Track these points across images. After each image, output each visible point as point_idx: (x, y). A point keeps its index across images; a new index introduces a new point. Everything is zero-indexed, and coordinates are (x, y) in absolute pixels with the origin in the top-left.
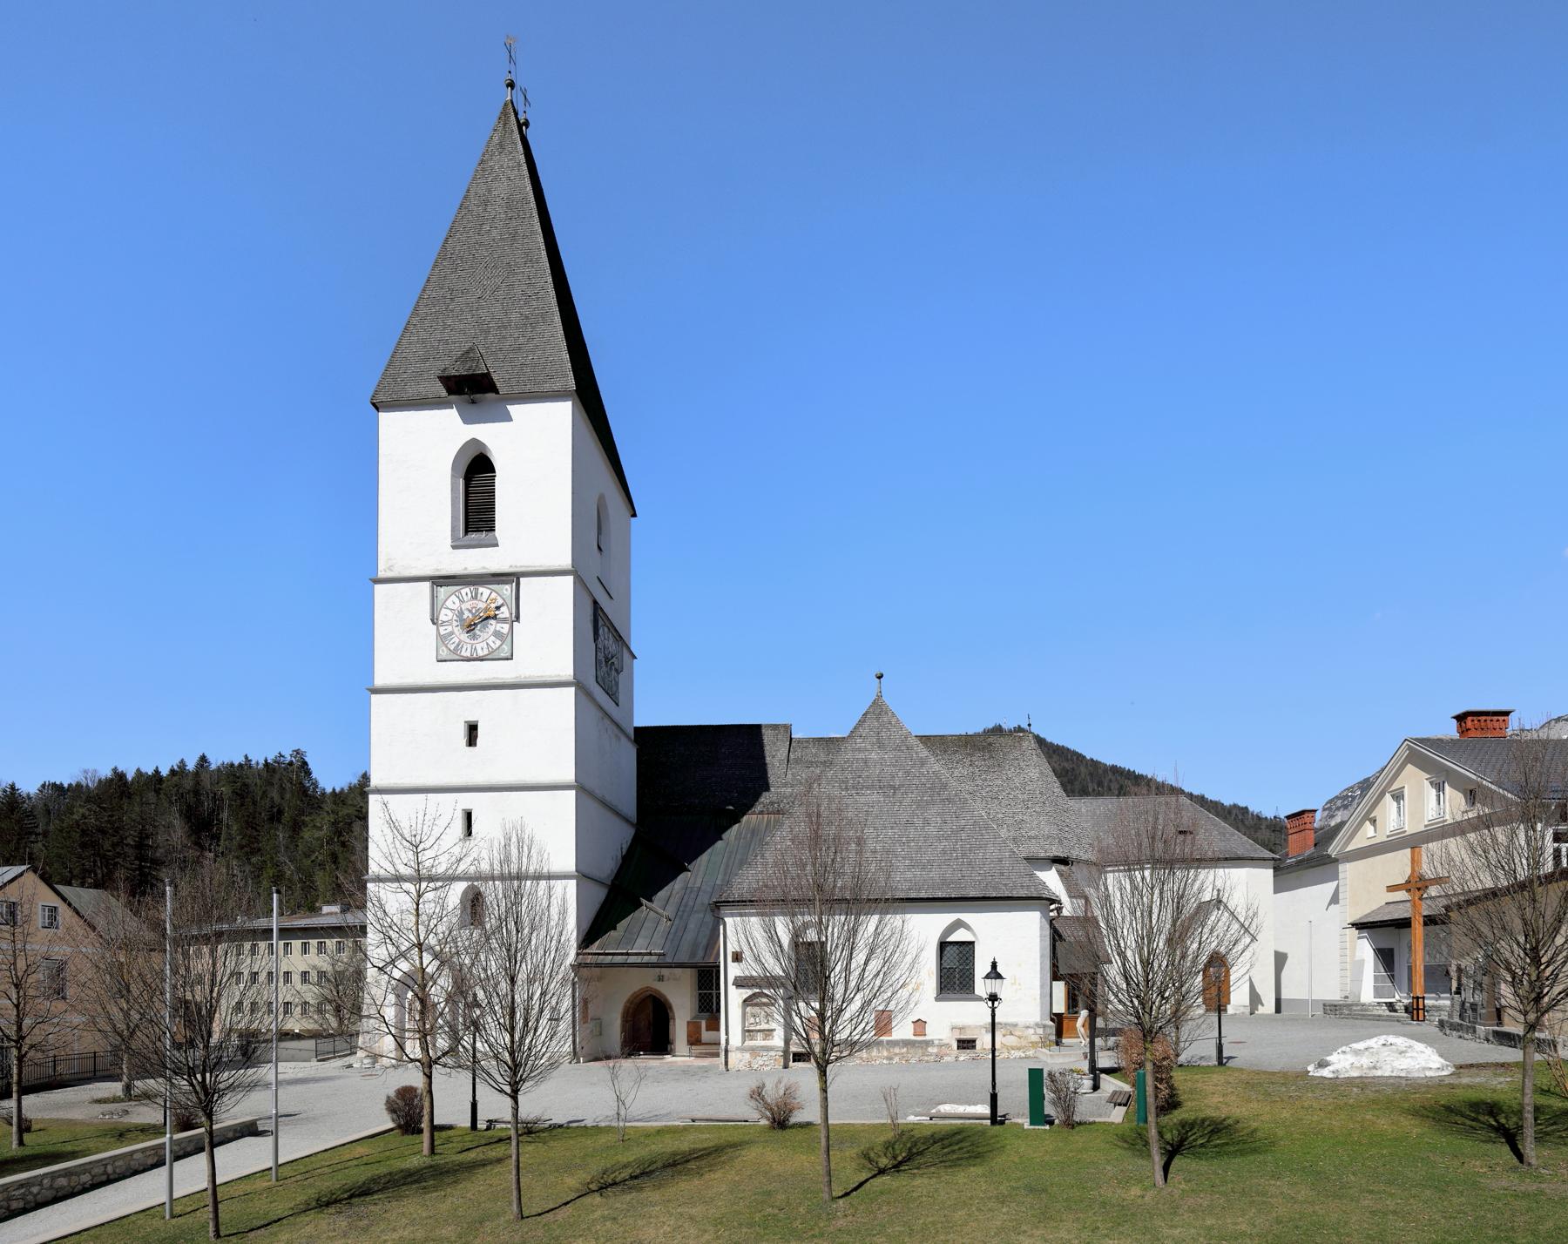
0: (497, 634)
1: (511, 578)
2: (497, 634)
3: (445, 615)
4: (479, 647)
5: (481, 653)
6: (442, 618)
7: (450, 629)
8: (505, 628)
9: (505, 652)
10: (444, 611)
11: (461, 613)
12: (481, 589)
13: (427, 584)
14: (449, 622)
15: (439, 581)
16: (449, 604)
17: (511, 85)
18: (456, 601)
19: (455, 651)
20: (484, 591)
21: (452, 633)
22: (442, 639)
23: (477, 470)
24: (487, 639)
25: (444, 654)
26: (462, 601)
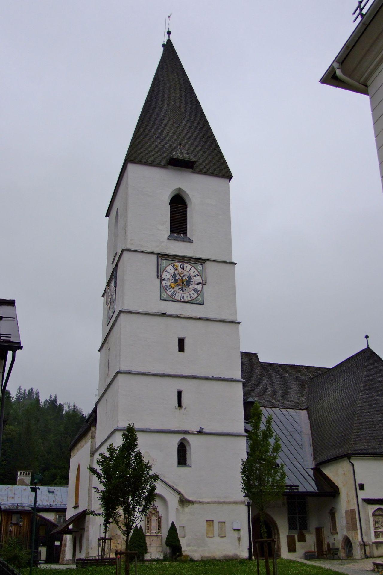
0: (195, 290)
1: (201, 261)
2: (195, 290)
3: (165, 275)
4: (185, 295)
5: (186, 300)
7: (168, 283)
8: (199, 288)
10: (165, 273)
11: (175, 276)
12: (186, 265)
13: (154, 257)
14: (168, 279)
16: (168, 269)
17: (169, 17)
18: (169, 270)
19: (171, 296)
20: (188, 266)
22: (163, 288)
23: (178, 204)
24: (189, 294)
25: (165, 296)
26: (175, 269)
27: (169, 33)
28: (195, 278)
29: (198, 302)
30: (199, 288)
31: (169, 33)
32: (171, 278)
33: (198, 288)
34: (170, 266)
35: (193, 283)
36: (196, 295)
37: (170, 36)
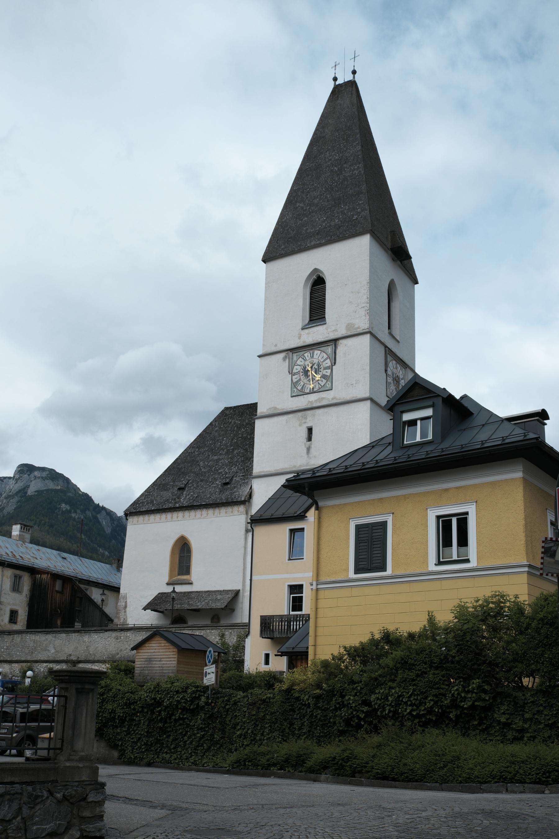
0: (324, 377)
6: (295, 371)
8: (328, 372)
9: (328, 386)
15: (293, 350)
16: (299, 362)
20: (317, 352)
21: (300, 379)
26: (305, 360)
27: (354, 72)
28: (324, 363)
29: (327, 389)
30: (328, 372)
31: (354, 72)
32: (302, 371)
33: (326, 374)
34: (301, 359)
35: (321, 370)
36: (325, 381)
37: (356, 75)
